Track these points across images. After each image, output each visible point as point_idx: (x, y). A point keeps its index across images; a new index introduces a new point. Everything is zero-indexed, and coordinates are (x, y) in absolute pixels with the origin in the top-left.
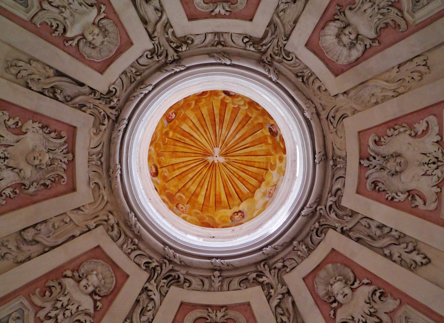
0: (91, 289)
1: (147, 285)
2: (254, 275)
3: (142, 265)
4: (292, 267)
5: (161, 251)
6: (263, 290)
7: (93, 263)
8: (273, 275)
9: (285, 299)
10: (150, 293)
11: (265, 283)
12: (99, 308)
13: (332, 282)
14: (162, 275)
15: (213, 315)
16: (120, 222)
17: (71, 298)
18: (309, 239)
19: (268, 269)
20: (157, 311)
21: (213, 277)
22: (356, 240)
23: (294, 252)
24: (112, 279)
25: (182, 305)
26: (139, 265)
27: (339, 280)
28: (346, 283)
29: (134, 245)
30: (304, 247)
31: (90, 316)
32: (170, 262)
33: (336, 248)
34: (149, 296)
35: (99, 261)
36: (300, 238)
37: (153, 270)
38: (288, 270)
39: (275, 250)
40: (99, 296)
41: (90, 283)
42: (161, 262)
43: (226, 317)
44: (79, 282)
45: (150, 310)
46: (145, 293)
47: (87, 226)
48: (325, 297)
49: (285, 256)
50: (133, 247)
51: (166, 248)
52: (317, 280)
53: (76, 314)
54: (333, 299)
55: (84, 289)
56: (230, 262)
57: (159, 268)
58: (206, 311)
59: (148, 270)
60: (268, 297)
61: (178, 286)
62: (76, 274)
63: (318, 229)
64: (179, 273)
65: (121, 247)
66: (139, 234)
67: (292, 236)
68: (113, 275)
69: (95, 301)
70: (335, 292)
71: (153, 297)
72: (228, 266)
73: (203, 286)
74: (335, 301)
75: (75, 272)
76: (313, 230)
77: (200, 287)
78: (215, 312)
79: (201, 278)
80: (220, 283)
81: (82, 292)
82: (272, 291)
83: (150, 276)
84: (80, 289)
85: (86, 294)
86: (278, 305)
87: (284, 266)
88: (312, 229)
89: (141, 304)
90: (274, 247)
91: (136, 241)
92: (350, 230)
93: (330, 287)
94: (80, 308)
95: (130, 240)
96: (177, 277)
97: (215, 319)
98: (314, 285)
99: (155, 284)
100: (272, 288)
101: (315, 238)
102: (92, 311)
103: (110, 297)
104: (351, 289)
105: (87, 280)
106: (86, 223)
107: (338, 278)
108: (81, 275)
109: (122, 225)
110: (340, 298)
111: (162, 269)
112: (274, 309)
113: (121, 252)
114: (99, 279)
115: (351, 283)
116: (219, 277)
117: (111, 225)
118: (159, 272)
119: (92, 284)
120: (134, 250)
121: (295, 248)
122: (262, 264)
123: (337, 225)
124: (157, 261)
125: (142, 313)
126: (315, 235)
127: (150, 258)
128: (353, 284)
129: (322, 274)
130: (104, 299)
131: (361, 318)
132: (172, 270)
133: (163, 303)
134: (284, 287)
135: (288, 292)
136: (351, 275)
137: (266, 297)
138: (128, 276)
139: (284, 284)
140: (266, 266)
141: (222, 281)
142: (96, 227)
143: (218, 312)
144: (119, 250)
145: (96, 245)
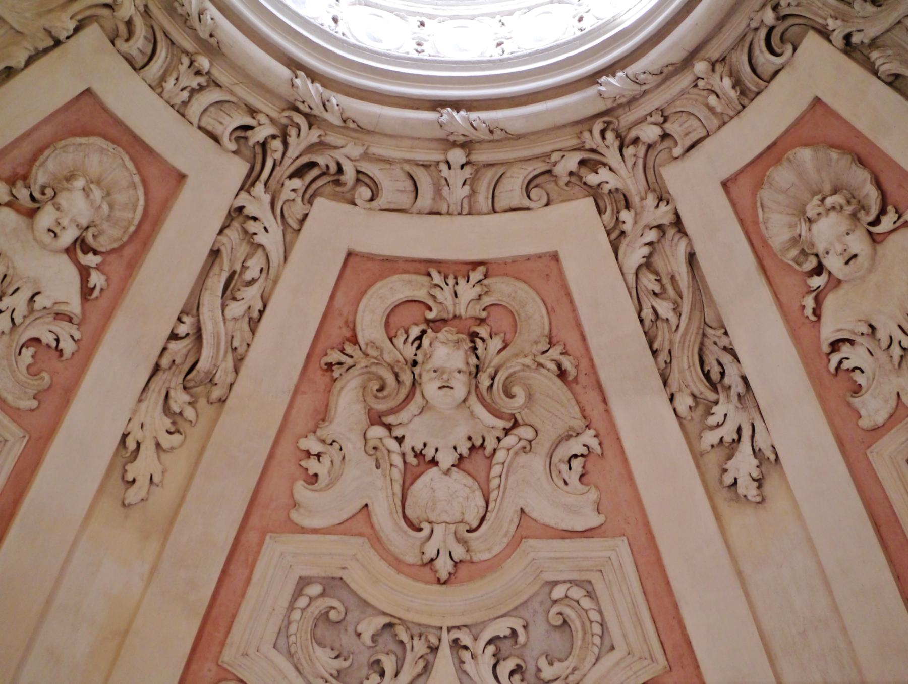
0: (68, 237)
1: (243, 200)
2: (571, 162)
3: (225, 139)
4: (688, 142)
5: (285, 90)
6: (600, 212)
7: (71, 149)
8: (630, 163)
9: (666, 242)
10: (252, 226)
11: (606, 188)
12: (96, 293)
13: (811, 213)
14: (287, 161)
15: (444, 297)
16: (152, 6)
17: (10, 272)
18: (745, 58)
19: (617, 144)
20: (275, 282)
21: (443, 167)
22: (890, 79)
23: (695, 90)
24: (131, 192)
25: (351, 259)
26: (216, 139)
27: (833, 208)
28: (854, 216)
29: (198, 73)
30: (727, 82)
31: (70, 320)
32: (312, 120)
33: (827, 99)
34: (249, 236)
35: (92, 140)
36: (714, 51)
37: (259, 150)
38: (677, 151)
39: (637, 87)
40: (95, 253)
41: (65, 222)
42: (284, 121)
43: (487, 301)
44: (31, 214)
45: (253, 281)
46: (236, 224)
47: (48, 32)
48: (788, 250)
49: (670, 103)
50: (195, 82)
51: (298, 82)
52: (765, 194)
53: (28, 321)
54: (811, 263)
55: (48, 238)
56: (497, 120)
57: (277, 144)
58: (425, 279)
59: (243, 149)
60: (614, 236)
61: (336, 197)
62: (22, 194)
63: (771, 29)
64: (338, 155)
65: (158, 87)
66: (212, 41)
67: (690, 45)
68: (137, 179)
69: (84, 272)
70: (820, 248)
71: (261, 238)
72: (491, 132)
73: (413, 195)
74: (819, 269)
75: (20, 183)
76: (756, 29)
77: (405, 200)
78: (451, 281)
79: (407, 167)
80: (467, 188)
81: (44, 246)
82: (625, 215)
83: (252, 168)
84: (35, 239)
85: (56, 252)
86: (647, 264)
87: (665, 136)
88: (754, 25)
89: (226, 266)
90: (635, 76)
91: (204, 62)
92: (874, 44)
93: (804, 227)
94: (40, 302)
95: (186, 61)
96: (333, 168)
97: (451, 308)
98: (755, 208)
99: (267, 198)
100: (628, 206)
101: (763, 58)
102: (75, 306)
103: (128, 252)
104: (870, 233)
105: (58, 209)
106: (45, 22)
107: (830, 201)
108: (37, 195)
109: (158, 12)
110: (833, 263)
111: (286, 144)
112: (631, 278)
113: (161, 103)
114: (92, 203)
115: (871, 218)
116: (462, 167)
117: (127, 19)
118: (278, 156)
119: (73, 220)
120: (201, 88)
121: (701, 83)
122: (598, 127)
123: (831, 24)
124: (272, 121)
125: (229, 291)
126: (764, 49)
127: (253, 111)
128: (876, 222)
129: (782, 175)
130: (111, 258)
131: (898, 335)
132: (321, 146)
133: (293, 257)
134: (663, 205)
135: (678, 222)
136: (872, 194)
137: (609, 233)
138: (182, 177)
139: (663, 198)
140: (610, 135)
141: (471, 183)
142: (77, 30)
143: (462, 281)
144: (153, 96)
145: (84, 88)
